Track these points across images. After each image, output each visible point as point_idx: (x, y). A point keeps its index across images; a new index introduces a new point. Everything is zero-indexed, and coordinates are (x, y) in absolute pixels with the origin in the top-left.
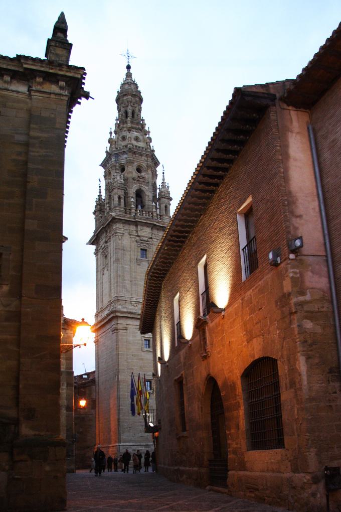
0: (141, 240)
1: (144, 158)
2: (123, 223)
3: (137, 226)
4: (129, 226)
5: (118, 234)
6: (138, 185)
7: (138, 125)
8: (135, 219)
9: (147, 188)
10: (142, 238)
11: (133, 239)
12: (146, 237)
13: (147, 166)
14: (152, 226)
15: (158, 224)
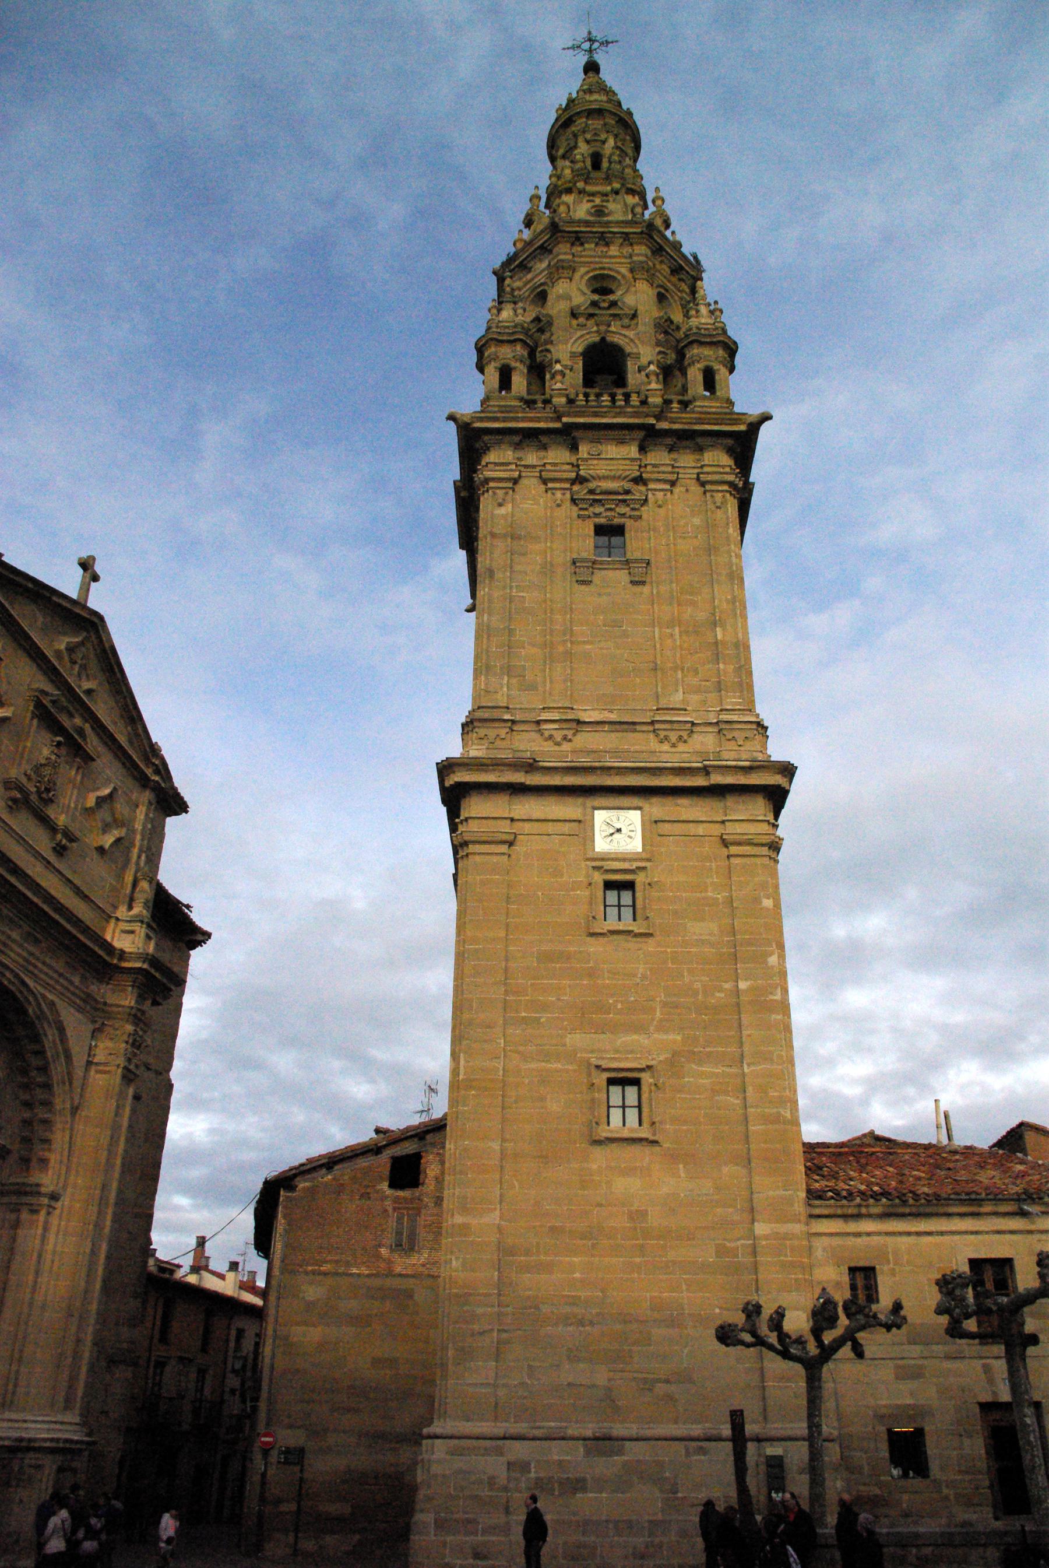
0: (591, 492)
1: (614, 250)
2: (517, 446)
3: (574, 448)
4: (542, 454)
5: (492, 484)
6: (595, 329)
7: (610, 184)
8: (558, 419)
9: (631, 334)
10: (592, 485)
11: (559, 495)
12: (614, 478)
13: (632, 271)
14: (641, 434)
15: (664, 425)
